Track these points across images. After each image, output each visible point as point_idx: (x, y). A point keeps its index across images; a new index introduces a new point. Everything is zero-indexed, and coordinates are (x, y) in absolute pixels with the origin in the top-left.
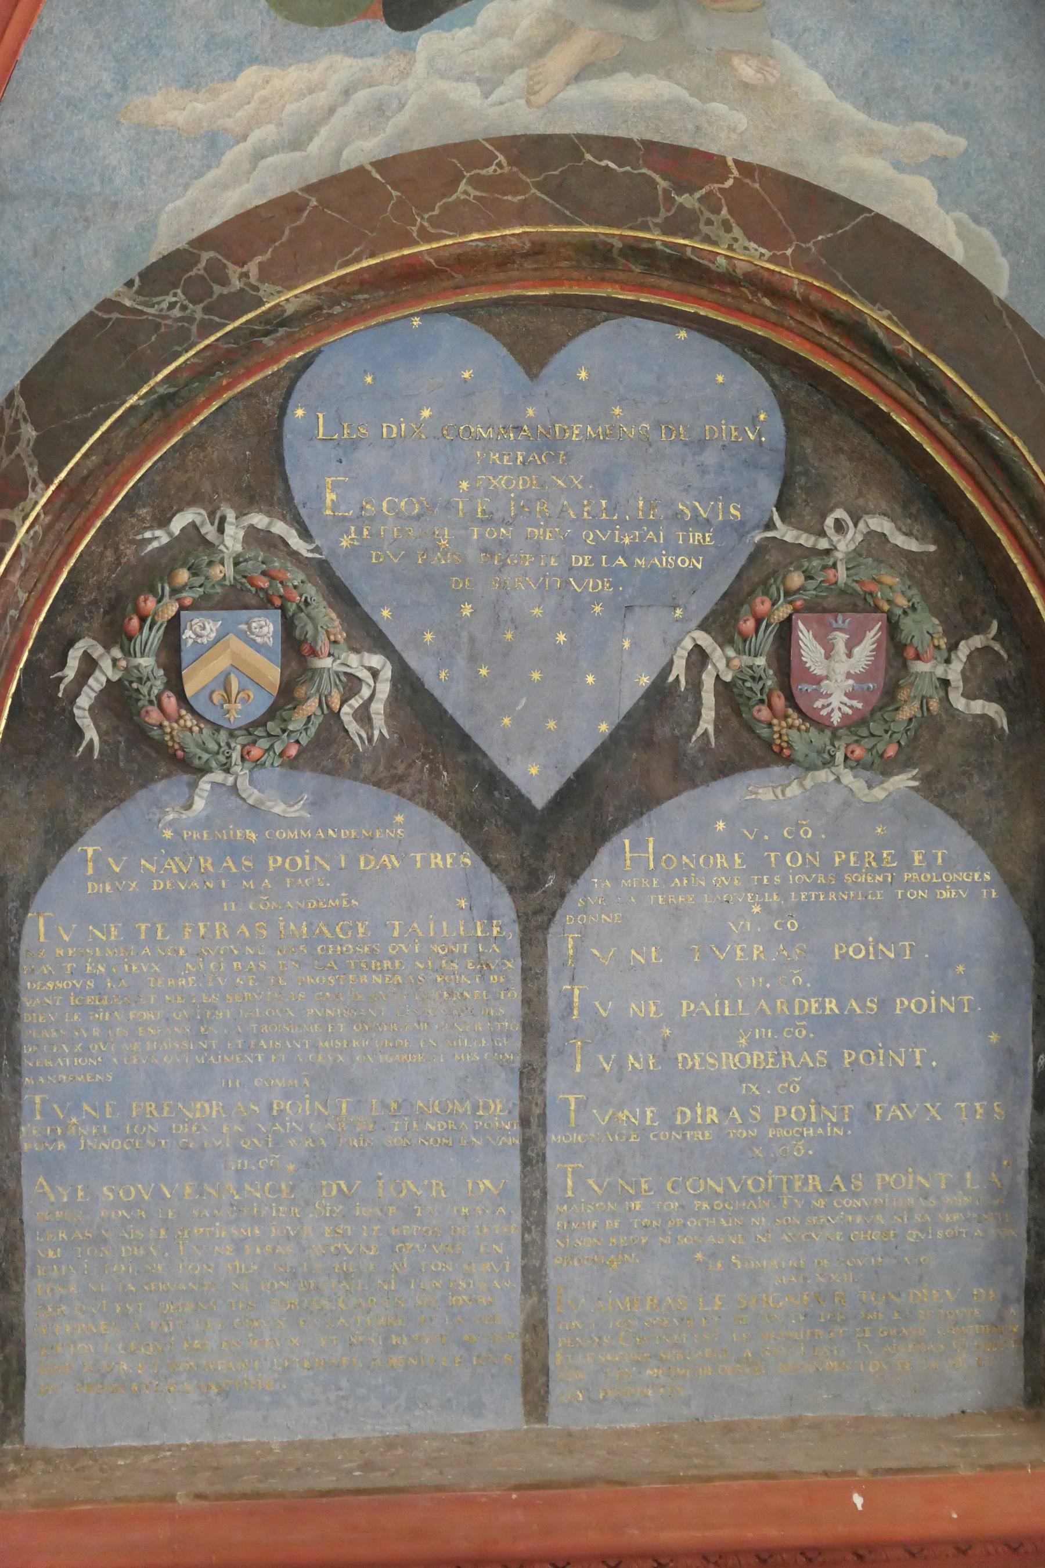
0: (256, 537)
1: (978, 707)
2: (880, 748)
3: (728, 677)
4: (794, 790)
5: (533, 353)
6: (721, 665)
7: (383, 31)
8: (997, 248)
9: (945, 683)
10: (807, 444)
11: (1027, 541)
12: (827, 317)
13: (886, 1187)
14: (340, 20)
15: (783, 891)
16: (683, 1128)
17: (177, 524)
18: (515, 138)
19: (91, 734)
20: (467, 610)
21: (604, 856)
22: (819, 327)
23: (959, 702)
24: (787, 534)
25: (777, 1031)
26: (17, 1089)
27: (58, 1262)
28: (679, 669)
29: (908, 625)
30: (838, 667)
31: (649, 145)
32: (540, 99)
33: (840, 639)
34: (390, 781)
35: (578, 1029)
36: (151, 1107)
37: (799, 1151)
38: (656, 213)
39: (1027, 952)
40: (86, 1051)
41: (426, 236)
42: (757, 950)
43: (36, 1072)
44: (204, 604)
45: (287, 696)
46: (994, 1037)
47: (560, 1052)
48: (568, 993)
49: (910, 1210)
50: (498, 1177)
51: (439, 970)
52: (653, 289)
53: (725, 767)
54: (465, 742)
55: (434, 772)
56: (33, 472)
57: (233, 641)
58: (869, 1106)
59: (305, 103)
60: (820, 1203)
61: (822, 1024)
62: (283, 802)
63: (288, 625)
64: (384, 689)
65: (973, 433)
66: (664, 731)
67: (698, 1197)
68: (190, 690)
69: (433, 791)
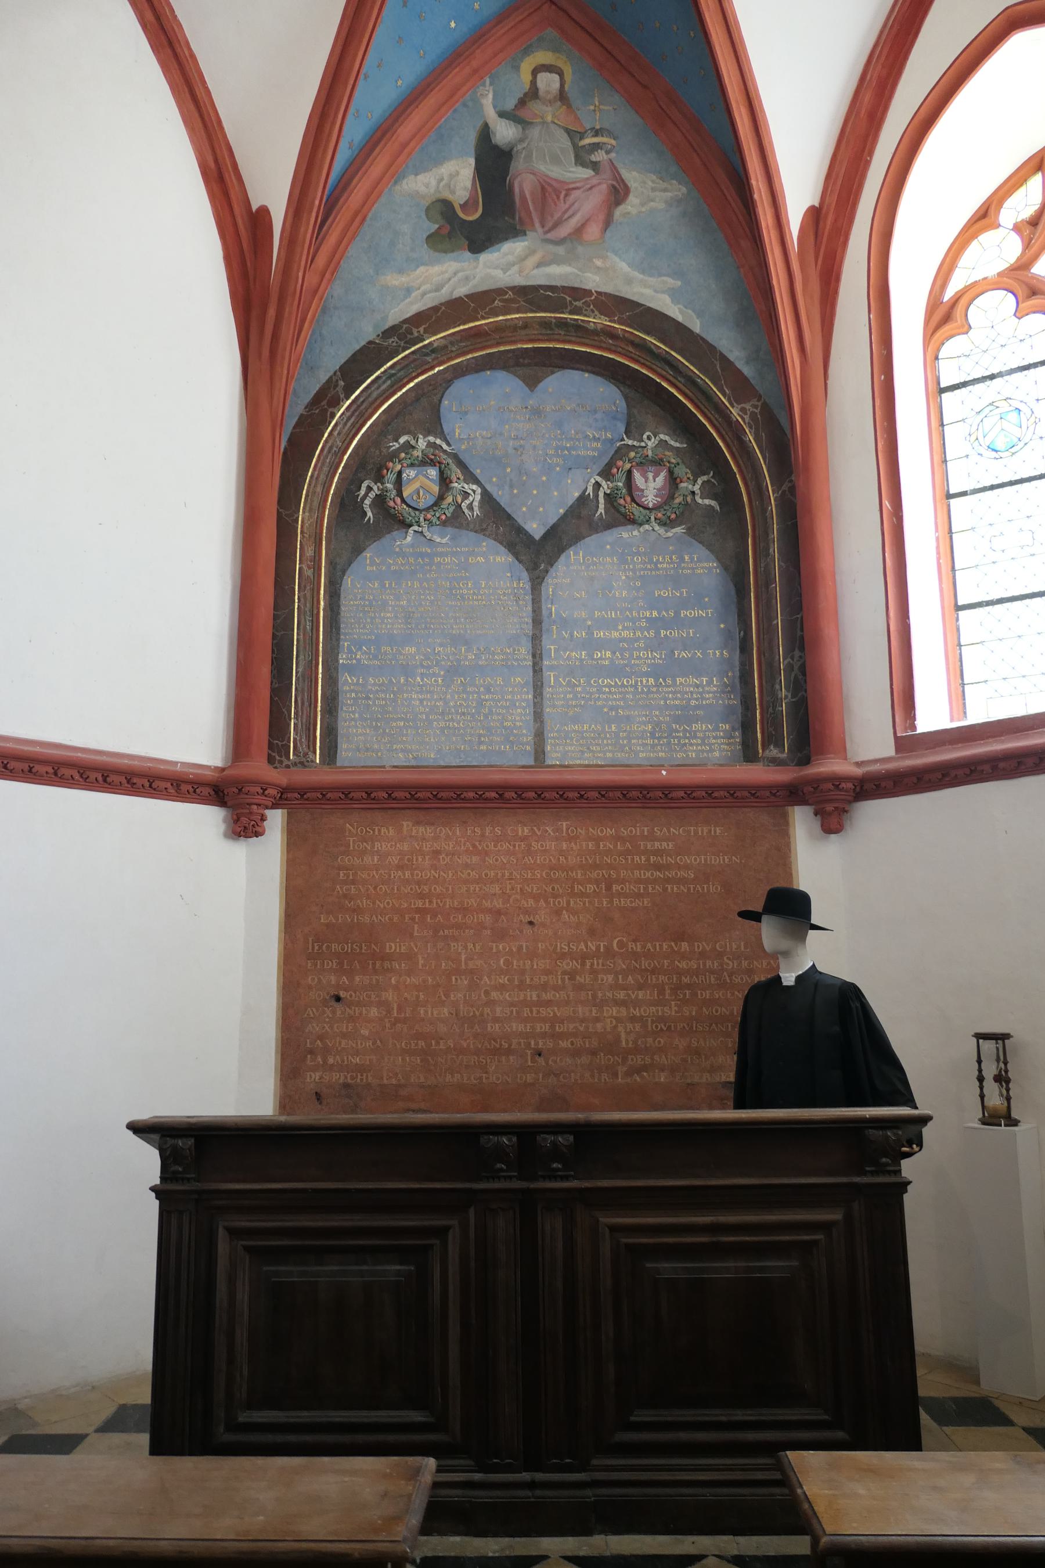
0: (430, 445)
1: (707, 502)
2: (669, 514)
3: (608, 492)
4: (635, 533)
5: (532, 383)
6: (606, 487)
7: (468, 254)
8: (695, 317)
9: (693, 493)
10: (635, 411)
11: (715, 422)
12: (632, 343)
13: (681, 683)
14: (453, 251)
15: (634, 571)
16: (597, 660)
17: (402, 440)
18: (515, 287)
19: (370, 514)
20: (509, 470)
21: (563, 557)
22: (631, 349)
23: (700, 501)
24: (630, 442)
25: (634, 623)
26: (338, 640)
27: (352, 705)
28: (590, 490)
29: (676, 471)
30: (651, 486)
31: (563, 287)
32: (524, 274)
33: (650, 475)
34: (482, 531)
35: (554, 621)
36: (389, 649)
37: (645, 669)
38: (566, 308)
39: (733, 592)
40: (364, 627)
41: (484, 318)
42: (624, 593)
43: (345, 634)
44: (412, 465)
45: (441, 497)
46: (722, 626)
47: (548, 630)
48: (551, 609)
49: (692, 693)
50: (523, 678)
51: (500, 599)
52: (570, 342)
53: (609, 526)
54: (509, 517)
55: (498, 528)
56: (342, 396)
57: (421, 477)
58: (673, 652)
59: (440, 278)
60: (654, 689)
61: (650, 620)
62: (441, 538)
63: (441, 473)
64: (478, 497)
65: (691, 381)
66: (584, 512)
67: (605, 686)
68: (405, 495)
69: (497, 535)
